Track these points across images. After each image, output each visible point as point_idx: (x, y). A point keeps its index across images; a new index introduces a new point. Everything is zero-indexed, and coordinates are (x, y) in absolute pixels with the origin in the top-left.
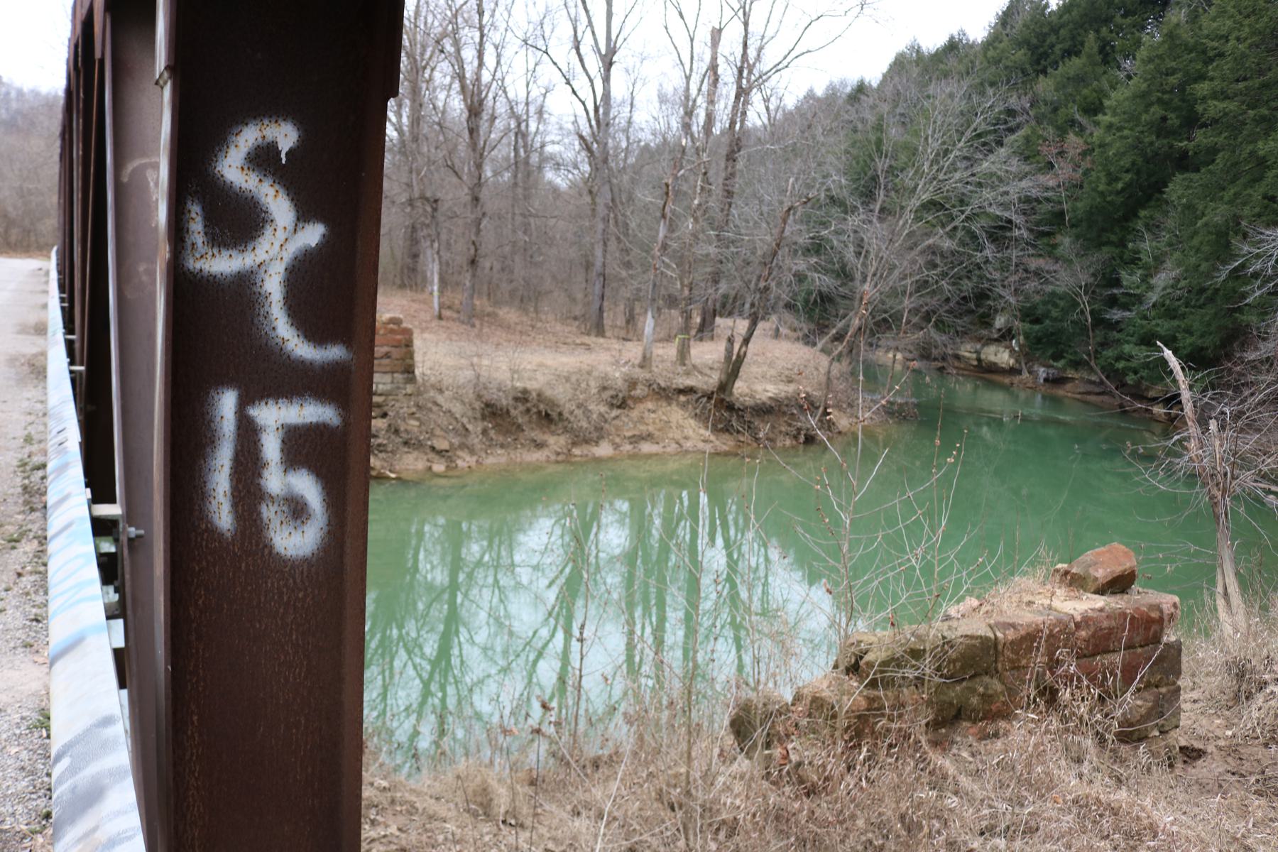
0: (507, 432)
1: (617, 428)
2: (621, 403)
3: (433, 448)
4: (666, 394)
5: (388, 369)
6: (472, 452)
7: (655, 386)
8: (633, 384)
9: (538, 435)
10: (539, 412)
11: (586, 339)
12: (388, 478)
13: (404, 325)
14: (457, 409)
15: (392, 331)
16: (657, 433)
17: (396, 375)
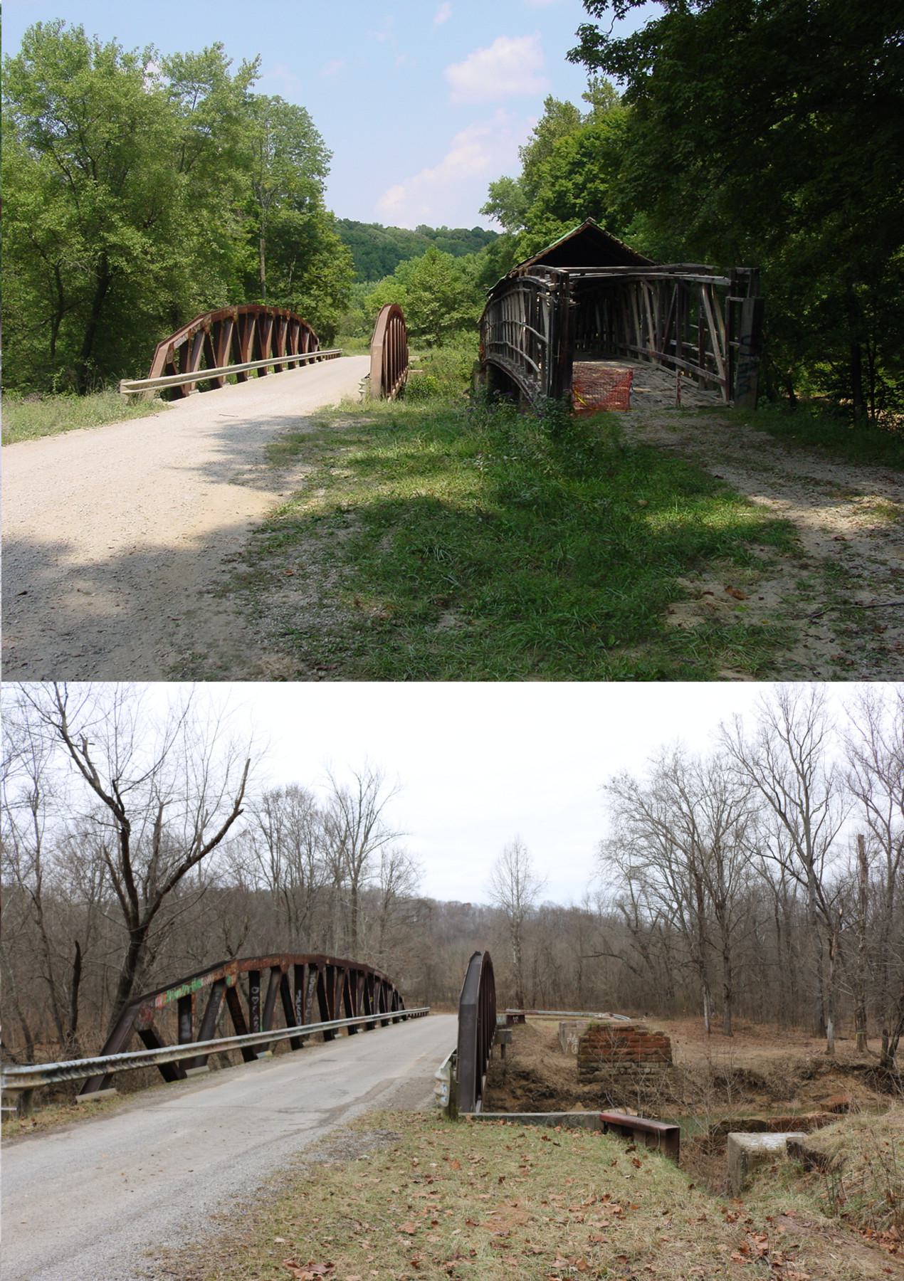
1: (806, 1091)
2: (811, 1074)
4: (844, 1070)
8: (818, 1064)
9: (750, 1096)
10: (750, 1083)
11: (812, 1041)
14: (699, 1081)
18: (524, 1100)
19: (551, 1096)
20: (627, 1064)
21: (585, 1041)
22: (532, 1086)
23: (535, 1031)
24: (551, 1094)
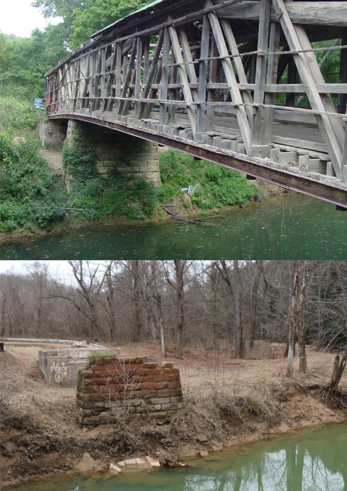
0: (234, 425)
3: (198, 441)
5: (167, 395)
6: (219, 440)
7: (298, 387)
8: (287, 386)
12: (181, 466)
13: (175, 367)
14: (204, 412)
15: (168, 372)
16: (306, 414)
17: (171, 398)
18: (17, 459)
19: (53, 449)
20: (137, 402)
21: (88, 376)
22: (28, 438)
23: (14, 358)
24: (53, 447)
